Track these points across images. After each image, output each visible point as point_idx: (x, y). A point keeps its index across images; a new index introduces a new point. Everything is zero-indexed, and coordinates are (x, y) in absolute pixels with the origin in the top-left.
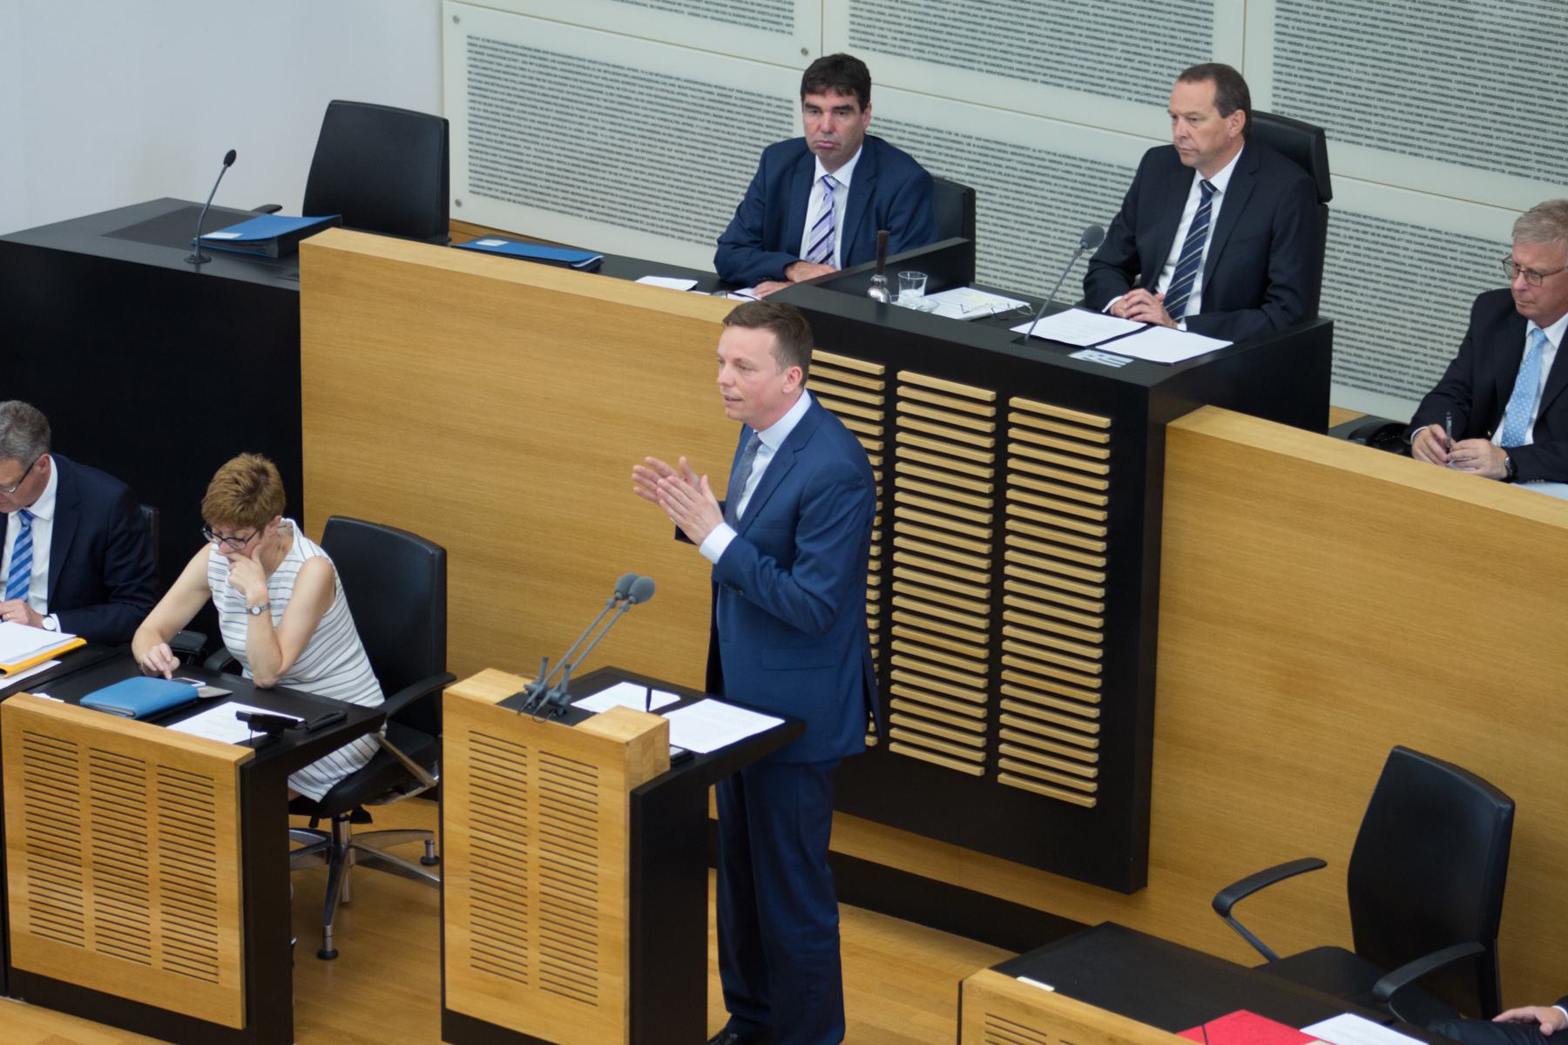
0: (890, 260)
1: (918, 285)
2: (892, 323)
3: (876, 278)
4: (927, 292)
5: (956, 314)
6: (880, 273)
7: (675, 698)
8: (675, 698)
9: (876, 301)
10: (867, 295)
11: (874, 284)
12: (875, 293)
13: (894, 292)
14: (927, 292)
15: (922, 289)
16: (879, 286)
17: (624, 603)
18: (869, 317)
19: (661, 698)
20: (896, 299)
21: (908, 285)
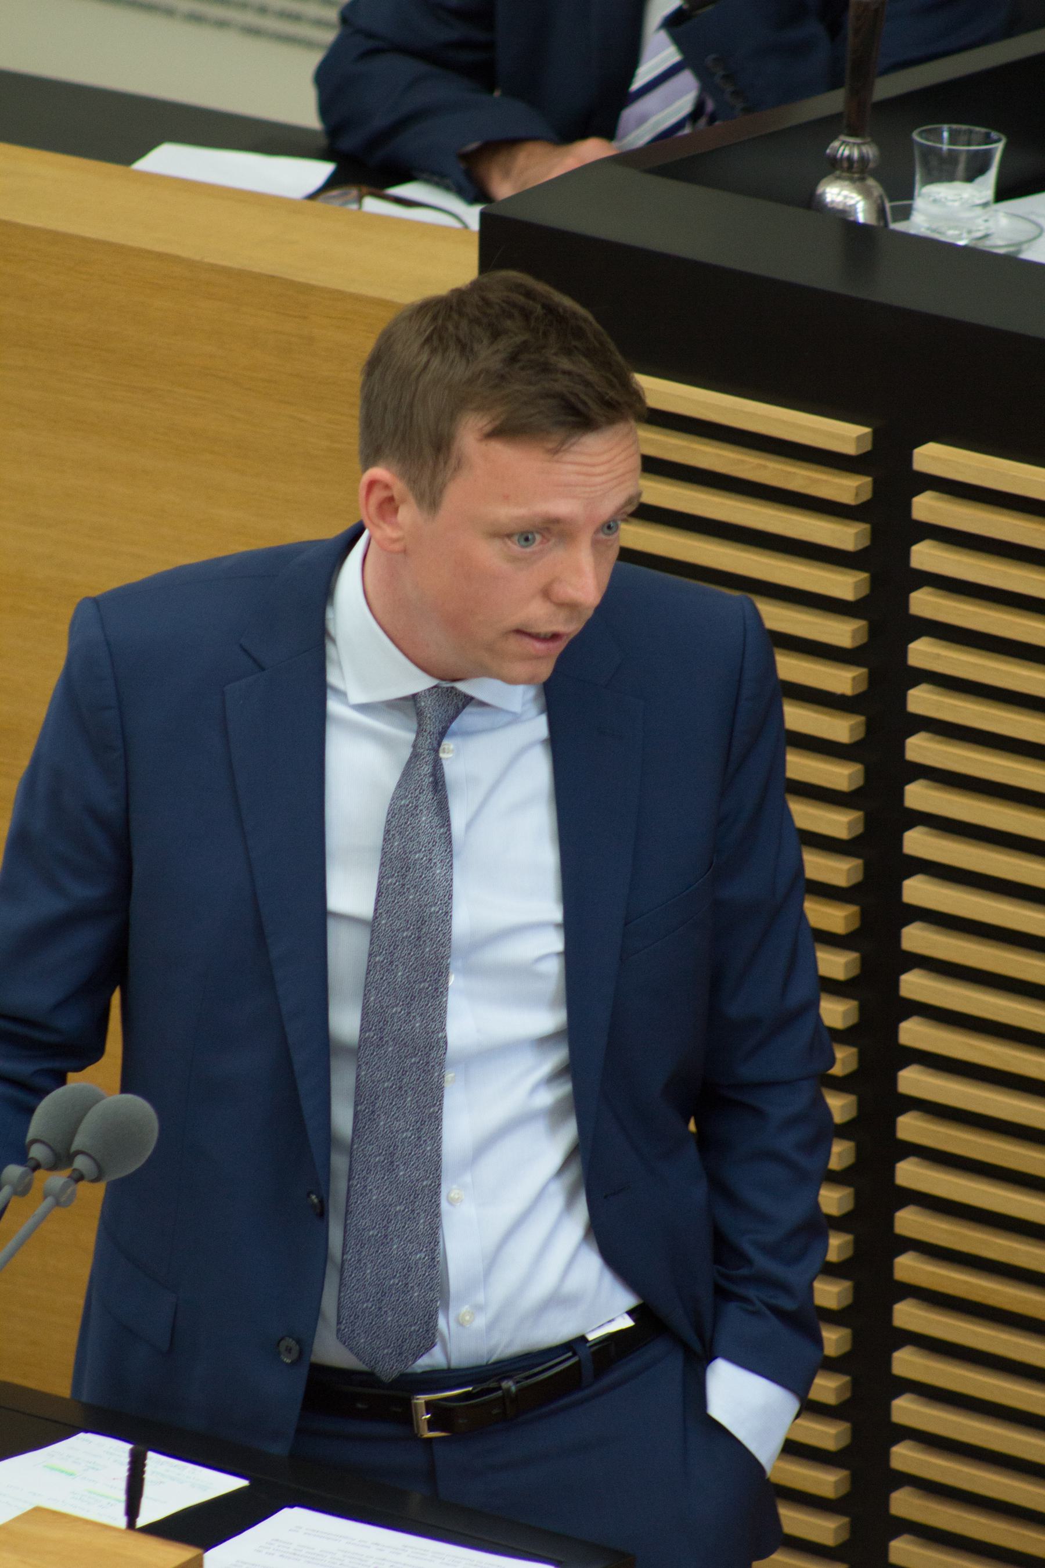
0: (887, 87)
1: (975, 170)
2: (895, 289)
3: (844, 148)
4: (1004, 192)
6: (854, 131)
7: (227, 1484)
8: (227, 1484)
9: (842, 218)
10: (813, 203)
11: (838, 168)
12: (837, 194)
14: (1004, 192)
15: (989, 180)
16: (853, 171)
17: (57, 1179)
18: (818, 270)
19: (180, 1484)
20: (905, 213)
21: (943, 170)
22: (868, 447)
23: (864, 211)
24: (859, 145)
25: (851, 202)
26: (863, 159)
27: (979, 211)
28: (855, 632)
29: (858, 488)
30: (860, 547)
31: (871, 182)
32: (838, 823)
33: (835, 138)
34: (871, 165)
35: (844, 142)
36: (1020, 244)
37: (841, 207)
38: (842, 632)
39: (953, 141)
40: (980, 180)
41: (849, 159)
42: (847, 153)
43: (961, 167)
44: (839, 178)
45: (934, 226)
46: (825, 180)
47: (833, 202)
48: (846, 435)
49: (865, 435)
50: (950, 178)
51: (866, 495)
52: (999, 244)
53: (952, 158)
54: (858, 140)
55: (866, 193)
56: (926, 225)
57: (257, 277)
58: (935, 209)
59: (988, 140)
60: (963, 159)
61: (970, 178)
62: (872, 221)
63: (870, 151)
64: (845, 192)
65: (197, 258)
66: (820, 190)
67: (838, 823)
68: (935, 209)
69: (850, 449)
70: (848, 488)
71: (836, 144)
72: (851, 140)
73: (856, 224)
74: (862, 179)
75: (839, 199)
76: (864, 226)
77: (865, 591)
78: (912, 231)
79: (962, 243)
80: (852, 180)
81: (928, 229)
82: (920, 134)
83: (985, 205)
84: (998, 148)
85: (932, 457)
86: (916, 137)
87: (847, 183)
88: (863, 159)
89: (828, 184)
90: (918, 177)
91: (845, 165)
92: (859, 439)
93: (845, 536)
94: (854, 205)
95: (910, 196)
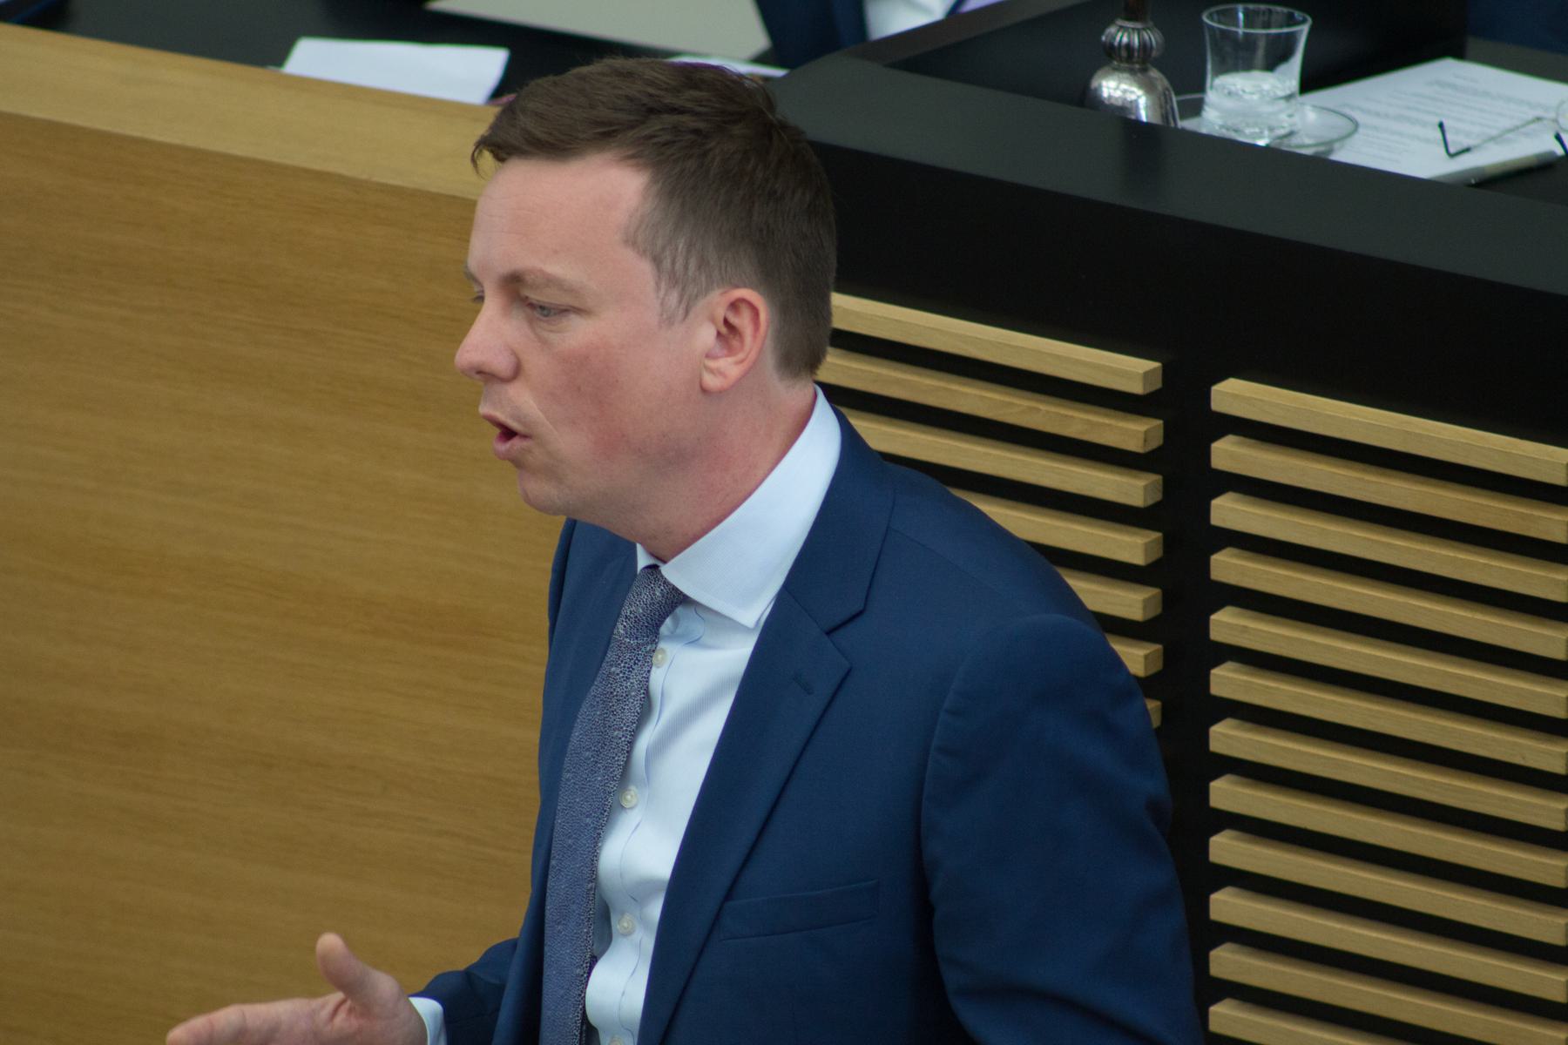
1: (1275, 57)
2: (1185, 199)
3: (1122, 34)
4: (1311, 81)
5: (1421, 160)
9: (1121, 116)
10: (1087, 99)
11: (1114, 58)
12: (1115, 88)
13: (1185, 82)
14: (1311, 81)
15: (1292, 70)
16: (1133, 61)
18: (1095, 179)
20: (1195, 108)
21: (1239, 57)
22: (1157, 384)
23: (1147, 108)
24: (1139, 31)
25: (1133, 97)
26: (1144, 47)
27: (1283, 104)
28: (1146, 602)
29: (1146, 432)
30: (1150, 502)
31: (1154, 73)
32: (1131, 602)
33: (1111, 22)
34: (1154, 54)
35: (1121, 27)
36: (1330, 144)
37: (1119, 103)
38: (1132, 546)
39: (1248, 24)
40: (1283, 68)
41: (1129, 47)
42: (1125, 40)
43: (1260, 53)
44: (1116, 69)
45: (1229, 123)
46: (1099, 73)
47: (1110, 97)
48: (1131, 371)
49: (1154, 370)
50: (1248, 66)
51: (1157, 441)
52: (1306, 144)
53: (1249, 43)
54: (1139, 25)
55: (1149, 87)
56: (1220, 122)
57: (434, 197)
58: (1229, 103)
59: (1291, 21)
60: (1262, 44)
61: (1271, 65)
62: (1156, 120)
63: (1153, 37)
64: (1124, 86)
65: (364, 177)
66: (1094, 84)
67: (1131, 602)
68: (1229, 103)
69: (1137, 388)
70: (1134, 433)
71: (1112, 29)
72: (1130, 25)
73: (1138, 123)
74: (1144, 70)
75: (1118, 94)
76: (1148, 125)
77: (1157, 553)
78: (1204, 131)
79: (1262, 143)
80: (1132, 72)
81: (1222, 127)
82: (1211, 17)
83: (1289, 98)
84: (1303, 31)
85: (1234, 395)
86: (1205, 19)
87: (1126, 75)
88: (1144, 47)
89: (1105, 76)
90: (1209, 67)
91: (1124, 54)
92: (1146, 375)
93: (1133, 489)
94: (1135, 103)
95: (1201, 87)
